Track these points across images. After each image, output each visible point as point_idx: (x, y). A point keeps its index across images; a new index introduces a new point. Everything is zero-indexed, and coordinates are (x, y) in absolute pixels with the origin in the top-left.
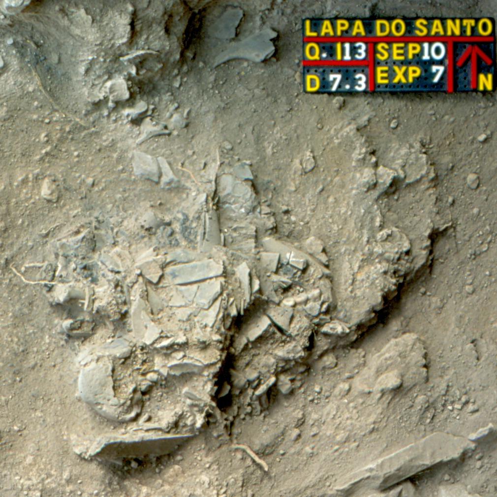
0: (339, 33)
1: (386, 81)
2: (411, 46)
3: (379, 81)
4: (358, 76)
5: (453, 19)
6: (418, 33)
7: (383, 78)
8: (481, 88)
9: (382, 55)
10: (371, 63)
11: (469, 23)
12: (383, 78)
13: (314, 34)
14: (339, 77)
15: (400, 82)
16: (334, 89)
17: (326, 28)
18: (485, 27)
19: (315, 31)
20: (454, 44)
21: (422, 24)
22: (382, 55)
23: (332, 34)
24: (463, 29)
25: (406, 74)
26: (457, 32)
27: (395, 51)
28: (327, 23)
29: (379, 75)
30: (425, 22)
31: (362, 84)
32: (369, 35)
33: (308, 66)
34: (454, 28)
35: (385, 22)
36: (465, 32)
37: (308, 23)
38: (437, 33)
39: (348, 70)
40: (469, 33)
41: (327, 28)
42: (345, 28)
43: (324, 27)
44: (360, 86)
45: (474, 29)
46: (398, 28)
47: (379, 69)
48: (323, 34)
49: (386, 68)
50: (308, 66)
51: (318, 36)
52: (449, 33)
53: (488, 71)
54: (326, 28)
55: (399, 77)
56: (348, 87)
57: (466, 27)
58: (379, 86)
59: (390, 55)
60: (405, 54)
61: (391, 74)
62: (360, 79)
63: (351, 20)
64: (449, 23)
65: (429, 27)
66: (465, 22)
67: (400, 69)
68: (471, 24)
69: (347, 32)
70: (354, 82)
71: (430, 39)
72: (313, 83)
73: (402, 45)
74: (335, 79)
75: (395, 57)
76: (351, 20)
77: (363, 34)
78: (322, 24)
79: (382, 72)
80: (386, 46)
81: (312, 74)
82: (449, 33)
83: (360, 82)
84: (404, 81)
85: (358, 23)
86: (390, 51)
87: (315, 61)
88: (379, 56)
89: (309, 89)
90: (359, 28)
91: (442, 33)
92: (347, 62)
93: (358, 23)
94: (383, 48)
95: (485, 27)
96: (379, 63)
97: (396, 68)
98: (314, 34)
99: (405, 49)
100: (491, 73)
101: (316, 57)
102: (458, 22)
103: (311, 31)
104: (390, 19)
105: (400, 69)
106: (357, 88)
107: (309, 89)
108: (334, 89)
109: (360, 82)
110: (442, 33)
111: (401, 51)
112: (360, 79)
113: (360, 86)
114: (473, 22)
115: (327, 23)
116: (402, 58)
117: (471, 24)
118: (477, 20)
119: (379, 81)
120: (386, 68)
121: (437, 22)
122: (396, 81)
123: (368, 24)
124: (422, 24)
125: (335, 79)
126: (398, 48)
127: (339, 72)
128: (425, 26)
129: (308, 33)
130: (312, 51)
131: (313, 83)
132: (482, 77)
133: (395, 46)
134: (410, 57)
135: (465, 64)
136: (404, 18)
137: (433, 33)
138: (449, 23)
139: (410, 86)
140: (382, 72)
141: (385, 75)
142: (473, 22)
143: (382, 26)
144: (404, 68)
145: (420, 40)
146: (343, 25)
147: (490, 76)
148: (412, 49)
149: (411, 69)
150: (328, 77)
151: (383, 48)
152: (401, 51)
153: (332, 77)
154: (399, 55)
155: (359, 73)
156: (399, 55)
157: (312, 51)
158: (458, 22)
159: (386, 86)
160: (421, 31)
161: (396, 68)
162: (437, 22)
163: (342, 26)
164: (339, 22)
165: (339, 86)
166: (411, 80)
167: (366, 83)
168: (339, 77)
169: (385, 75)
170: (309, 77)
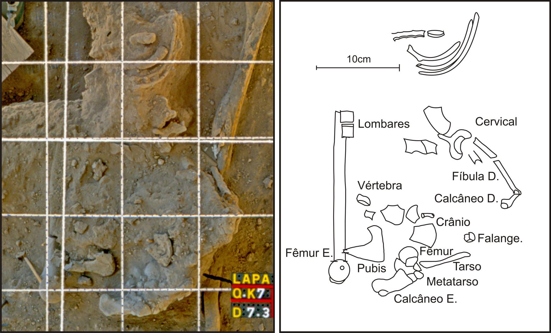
0: (254, 283)
4: (264, 309)
13: (239, 283)
14: (253, 309)
19: (239, 281)
28: (246, 276)
42: (258, 279)
43: (245, 278)
44: (266, 315)
62: (266, 311)
70: (262, 313)
78: (243, 276)
81: (236, 307)
83: (266, 313)
85: (266, 276)
87: (239, 299)
101: (239, 297)
106: (264, 316)
108: (250, 315)
109: (266, 313)
112: (266, 311)
113: (266, 315)
125: (250, 310)
131: (237, 313)
146: (256, 277)
150: (246, 308)
153: (248, 309)
155: (265, 307)
164: (254, 275)
165: (254, 314)
168: (253, 309)
170: (235, 309)
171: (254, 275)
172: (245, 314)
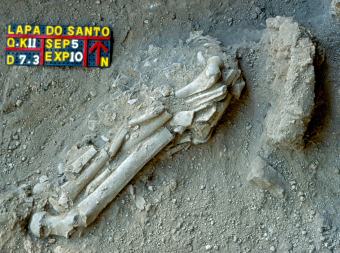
0: (26, 33)
1: (50, 60)
2: (65, 41)
3: (47, 60)
4: (35, 56)
5: (89, 27)
6: (69, 34)
7: (48, 58)
8: (102, 65)
9: (49, 45)
10: (42, 49)
11: (97, 29)
12: (48, 58)
13: (13, 33)
14: (24, 57)
15: (58, 60)
16: (22, 63)
17: (19, 30)
18: (105, 32)
20: (89, 39)
21: (71, 29)
22: (49, 45)
23: (22, 33)
24: (93, 32)
25: (61, 56)
26: (90, 34)
27: (56, 44)
28: (20, 27)
29: (47, 56)
30: (73, 28)
31: (37, 62)
32: (43, 34)
33: (8, 51)
34: (88, 31)
35: (52, 28)
36: (95, 34)
37: (10, 27)
38: (79, 34)
39: (30, 54)
40: (97, 35)
41: (20, 30)
42: (30, 30)
44: (36, 62)
45: (99, 33)
46: (58, 31)
47: (47, 53)
48: (17, 33)
49: (50, 53)
50: (8, 51)
51: (15, 34)
52: (86, 34)
53: (107, 56)
54: (19, 30)
55: (58, 57)
56: (29, 62)
58: (47, 63)
59: (53, 46)
60: (61, 45)
61: (53, 56)
62: (36, 58)
63: (33, 26)
64: (86, 29)
65: (75, 31)
66: (95, 28)
67: (58, 53)
69: (31, 32)
70: (33, 60)
71: (74, 37)
72: (10, 60)
73: (60, 40)
74: (22, 58)
75: (56, 47)
76: (33, 26)
77: (39, 33)
79: (48, 55)
80: (51, 41)
81: (11, 55)
82: (86, 34)
83: (36, 60)
84: (60, 60)
85: (37, 27)
86: (53, 43)
88: (47, 46)
89: (8, 63)
90: (37, 30)
91: (82, 34)
92: (30, 48)
93: (37, 27)
94: (49, 41)
95: (105, 32)
96: (47, 50)
97: (56, 53)
98: (13, 33)
99: (61, 42)
101: (13, 46)
102: (91, 28)
103: (11, 31)
104: (54, 26)
105: (58, 53)
106: (34, 63)
107: (8, 63)
108: (22, 63)
110: (82, 34)
111: (59, 44)
112: (36, 58)
113: (36, 62)
114: (99, 29)
115: (20, 27)
116: (59, 47)
119: (47, 60)
120: (50, 53)
121: (80, 28)
122: (56, 60)
123: (43, 29)
124: (71, 29)
125: (22, 58)
126: (58, 42)
127: (25, 54)
128: (73, 30)
129: (10, 32)
130: (11, 42)
131: (10, 60)
132: (103, 59)
133: (56, 41)
134: (64, 47)
135: (94, 51)
136: (62, 26)
137: (77, 34)
138: (86, 29)
139: (64, 63)
140: (48, 55)
141: (50, 56)
143: (50, 30)
144: (60, 53)
145: (70, 38)
146: (28, 28)
147: (107, 59)
148: (66, 43)
149: (64, 53)
150: (19, 57)
151: (49, 41)
152: (59, 44)
153: (21, 57)
154: (58, 45)
156: (58, 45)
157: (11, 42)
158: (91, 28)
159: (51, 63)
160: (71, 33)
161: (56, 53)
162: (80, 28)
163: (28, 28)
165: (25, 62)
166: (64, 60)
167: (39, 60)
168: (24, 57)
169: (50, 56)
170: (8, 56)
171: (26, 27)
172: (17, 62)
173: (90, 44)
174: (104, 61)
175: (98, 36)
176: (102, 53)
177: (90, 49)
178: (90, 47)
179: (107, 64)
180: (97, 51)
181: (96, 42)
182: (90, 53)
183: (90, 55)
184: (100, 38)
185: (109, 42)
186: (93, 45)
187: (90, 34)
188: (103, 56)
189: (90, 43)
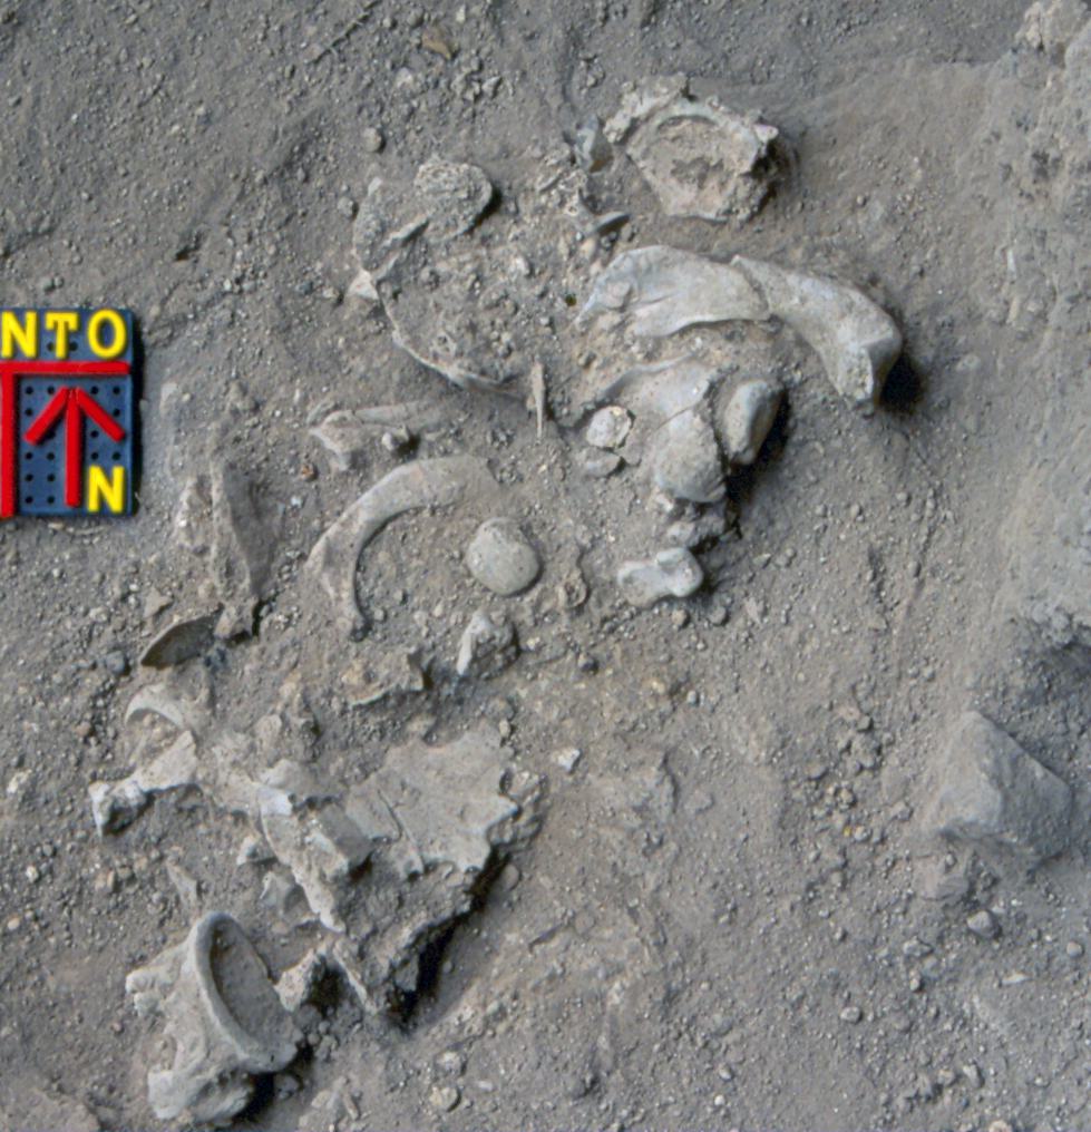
5: (19, 315)
8: (93, 505)
18: (105, 332)
24: (44, 337)
26: (29, 349)
36: (51, 347)
40: (60, 351)
45: (74, 341)
53: (117, 456)
57: (54, 331)
68: (66, 324)
95: (105, 332)
100: (122, 464)
102: (31, 318)
117: (66, 324)
118: (84, 315)
132: (95, 477)
135: (48, 434)
142: (72, 320)
147: (118, 473)
158: (31, 318)
173: (26, 402)
174: (106, 487)
175: (68, 356)
176: (94, 445)
177: (28, 424)
178: (29, 412)
179: (115, 502)
180: (63, 436)
181: (59, 386)
182: (27, 446)
183: (29, 456)
184: (77, 367)
185: (127, 386)
186: (41, 403)
187: (29, 349)
188: (95, 456)
189: (30, 391)
